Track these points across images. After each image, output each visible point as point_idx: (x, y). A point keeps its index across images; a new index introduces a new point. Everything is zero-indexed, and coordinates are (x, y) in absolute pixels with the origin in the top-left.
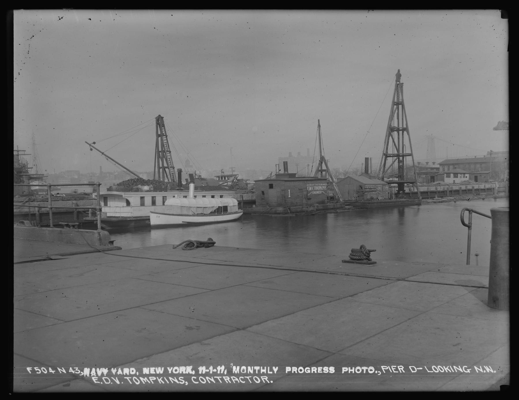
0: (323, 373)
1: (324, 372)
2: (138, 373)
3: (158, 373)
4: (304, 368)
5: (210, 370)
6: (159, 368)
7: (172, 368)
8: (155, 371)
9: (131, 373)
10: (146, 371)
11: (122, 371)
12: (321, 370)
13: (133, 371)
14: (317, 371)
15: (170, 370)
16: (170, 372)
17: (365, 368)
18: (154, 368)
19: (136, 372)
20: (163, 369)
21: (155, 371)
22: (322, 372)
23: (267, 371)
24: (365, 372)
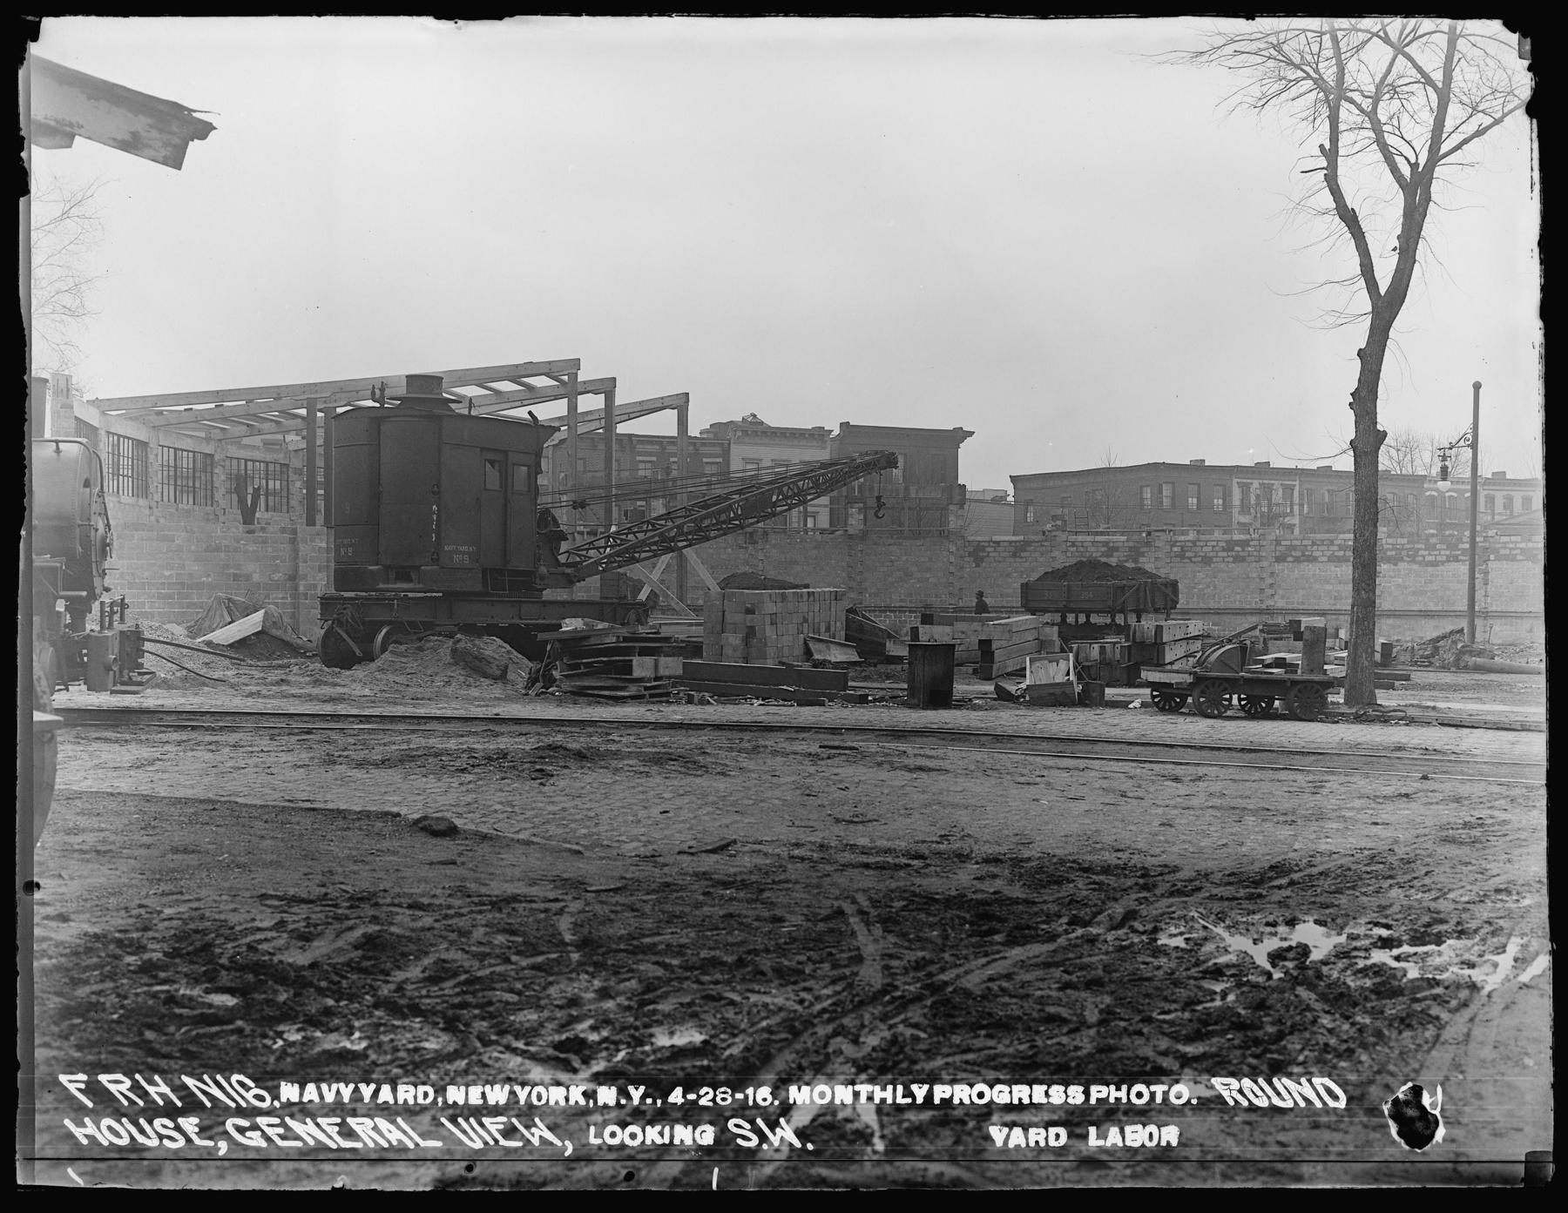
1: (1051, 1100)
2: (440, 1100)
3: (491, 1102)
4: (991, 1087)
6: (497, 1087)
7: (528, 1089)
8: (483, 1095)
10: (455, 1094)
13: (426, 1095)
14: (1030, 1096)
15: (522, 1094)
16: (522, 1102)
17: (1159, 1089)
19: (435, 1098)
20: (507, 1087)
21: (483, 1095)
22: (1044, 1101)
23: (895, 1098)
24: (1159, 1099)
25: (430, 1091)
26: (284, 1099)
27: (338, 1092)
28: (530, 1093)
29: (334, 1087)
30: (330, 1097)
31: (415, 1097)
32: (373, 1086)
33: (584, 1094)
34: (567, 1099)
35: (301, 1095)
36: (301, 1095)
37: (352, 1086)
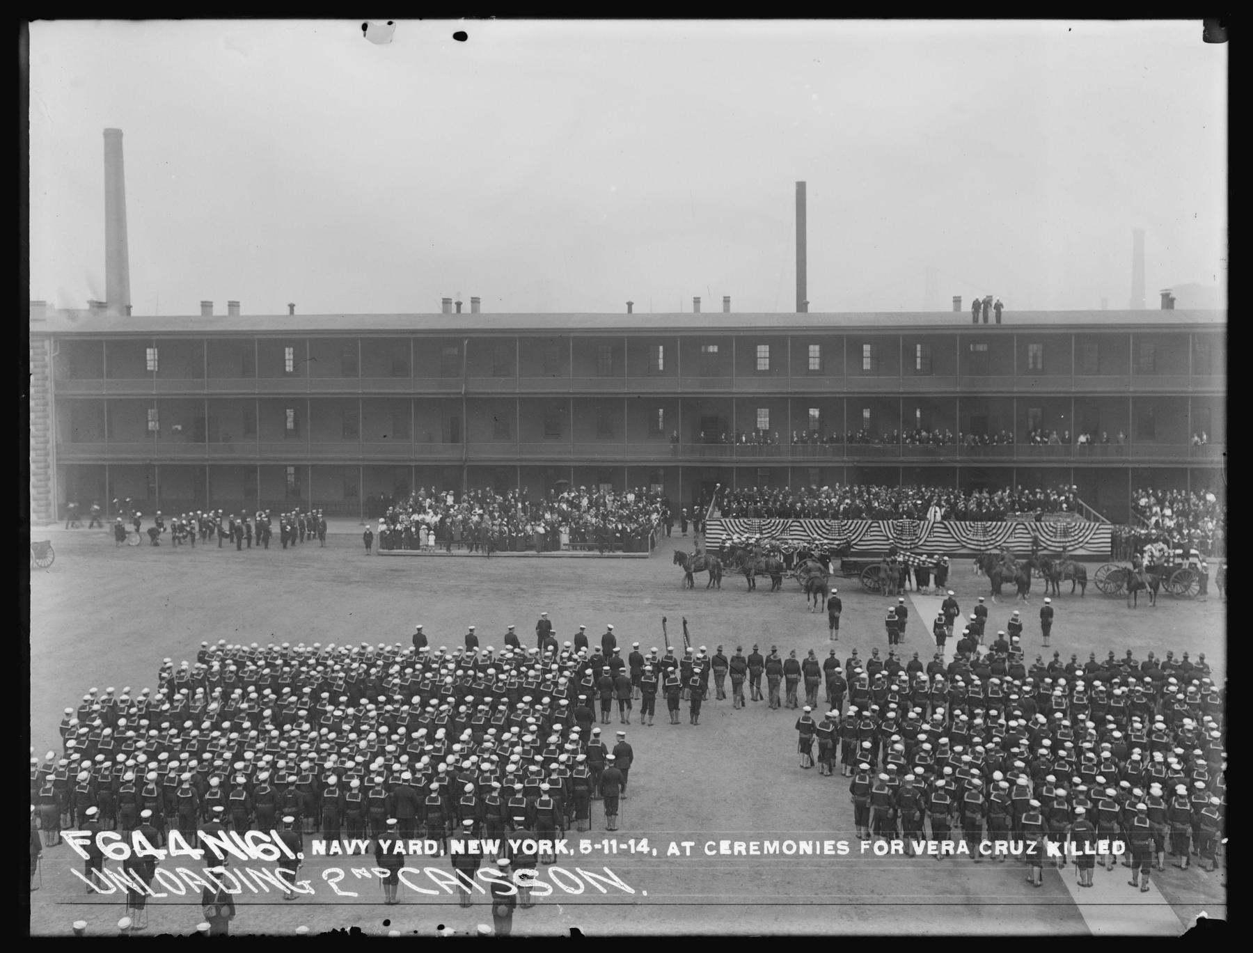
0: (837, 856)
1: (839, 852)
5: (603, 846)
6: (490, 842)
7: (519, 841)
8: (480, 847)
9: (427, 852)
11: (406, 846)
12: (831, 847)
13: (431, 847)
15: (515, 846)
18: (477, 842)
19: (439, 849)
20: (498, 842)
21: (480, 847)
25: (434, 843)
26: (314, 853)
27: (357, 847)
28: (521, 844)
29: (354, 842)
30: (350, 851)
31: (423, 848)
32: (389, 842)
33: (565, 845)
34: (553, 847)
35: (328, 848)
36: (328, 848)
37: (367, 842)
